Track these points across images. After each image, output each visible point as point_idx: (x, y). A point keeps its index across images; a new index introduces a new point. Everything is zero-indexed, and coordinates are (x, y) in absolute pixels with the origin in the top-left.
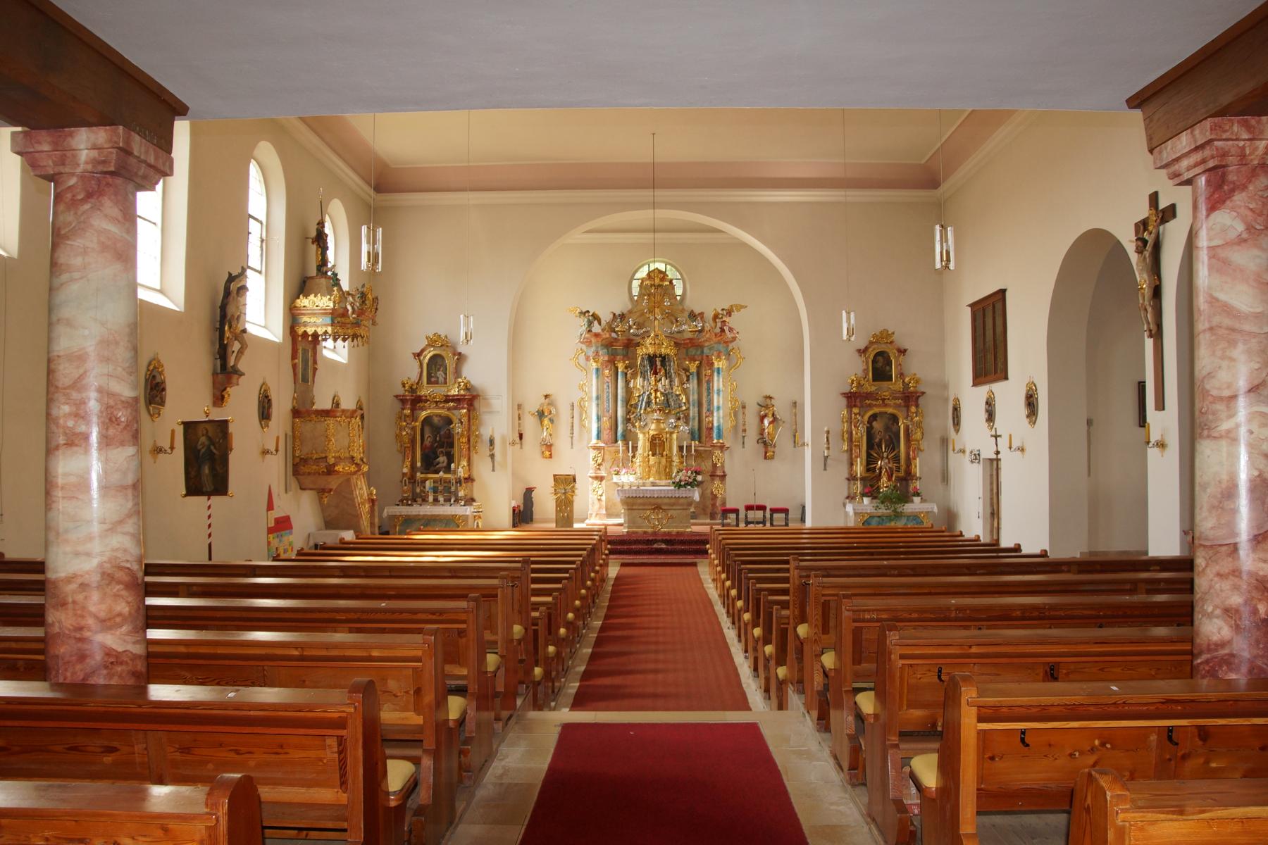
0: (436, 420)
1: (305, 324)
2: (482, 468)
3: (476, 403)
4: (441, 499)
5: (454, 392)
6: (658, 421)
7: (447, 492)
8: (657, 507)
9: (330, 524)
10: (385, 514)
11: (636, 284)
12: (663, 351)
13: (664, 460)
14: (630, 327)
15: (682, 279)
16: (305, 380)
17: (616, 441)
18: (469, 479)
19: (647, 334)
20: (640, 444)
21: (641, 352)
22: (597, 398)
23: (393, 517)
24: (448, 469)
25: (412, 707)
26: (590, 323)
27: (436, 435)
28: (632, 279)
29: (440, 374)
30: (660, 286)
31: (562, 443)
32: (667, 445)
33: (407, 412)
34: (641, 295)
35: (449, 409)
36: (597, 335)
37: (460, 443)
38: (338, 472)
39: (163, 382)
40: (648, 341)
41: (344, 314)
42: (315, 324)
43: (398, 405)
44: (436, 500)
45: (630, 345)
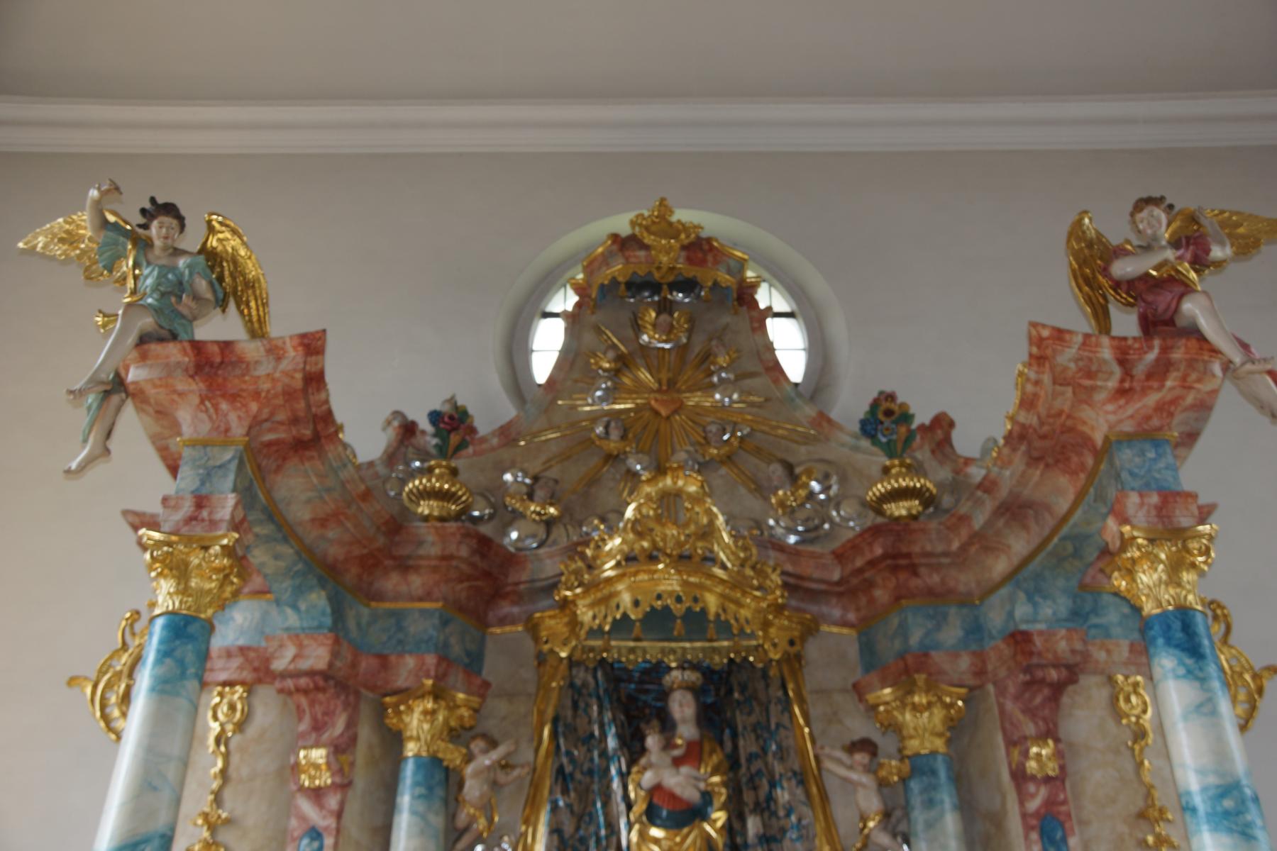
15: (806, 311)
34: (569, 359)
36: (212, 365)
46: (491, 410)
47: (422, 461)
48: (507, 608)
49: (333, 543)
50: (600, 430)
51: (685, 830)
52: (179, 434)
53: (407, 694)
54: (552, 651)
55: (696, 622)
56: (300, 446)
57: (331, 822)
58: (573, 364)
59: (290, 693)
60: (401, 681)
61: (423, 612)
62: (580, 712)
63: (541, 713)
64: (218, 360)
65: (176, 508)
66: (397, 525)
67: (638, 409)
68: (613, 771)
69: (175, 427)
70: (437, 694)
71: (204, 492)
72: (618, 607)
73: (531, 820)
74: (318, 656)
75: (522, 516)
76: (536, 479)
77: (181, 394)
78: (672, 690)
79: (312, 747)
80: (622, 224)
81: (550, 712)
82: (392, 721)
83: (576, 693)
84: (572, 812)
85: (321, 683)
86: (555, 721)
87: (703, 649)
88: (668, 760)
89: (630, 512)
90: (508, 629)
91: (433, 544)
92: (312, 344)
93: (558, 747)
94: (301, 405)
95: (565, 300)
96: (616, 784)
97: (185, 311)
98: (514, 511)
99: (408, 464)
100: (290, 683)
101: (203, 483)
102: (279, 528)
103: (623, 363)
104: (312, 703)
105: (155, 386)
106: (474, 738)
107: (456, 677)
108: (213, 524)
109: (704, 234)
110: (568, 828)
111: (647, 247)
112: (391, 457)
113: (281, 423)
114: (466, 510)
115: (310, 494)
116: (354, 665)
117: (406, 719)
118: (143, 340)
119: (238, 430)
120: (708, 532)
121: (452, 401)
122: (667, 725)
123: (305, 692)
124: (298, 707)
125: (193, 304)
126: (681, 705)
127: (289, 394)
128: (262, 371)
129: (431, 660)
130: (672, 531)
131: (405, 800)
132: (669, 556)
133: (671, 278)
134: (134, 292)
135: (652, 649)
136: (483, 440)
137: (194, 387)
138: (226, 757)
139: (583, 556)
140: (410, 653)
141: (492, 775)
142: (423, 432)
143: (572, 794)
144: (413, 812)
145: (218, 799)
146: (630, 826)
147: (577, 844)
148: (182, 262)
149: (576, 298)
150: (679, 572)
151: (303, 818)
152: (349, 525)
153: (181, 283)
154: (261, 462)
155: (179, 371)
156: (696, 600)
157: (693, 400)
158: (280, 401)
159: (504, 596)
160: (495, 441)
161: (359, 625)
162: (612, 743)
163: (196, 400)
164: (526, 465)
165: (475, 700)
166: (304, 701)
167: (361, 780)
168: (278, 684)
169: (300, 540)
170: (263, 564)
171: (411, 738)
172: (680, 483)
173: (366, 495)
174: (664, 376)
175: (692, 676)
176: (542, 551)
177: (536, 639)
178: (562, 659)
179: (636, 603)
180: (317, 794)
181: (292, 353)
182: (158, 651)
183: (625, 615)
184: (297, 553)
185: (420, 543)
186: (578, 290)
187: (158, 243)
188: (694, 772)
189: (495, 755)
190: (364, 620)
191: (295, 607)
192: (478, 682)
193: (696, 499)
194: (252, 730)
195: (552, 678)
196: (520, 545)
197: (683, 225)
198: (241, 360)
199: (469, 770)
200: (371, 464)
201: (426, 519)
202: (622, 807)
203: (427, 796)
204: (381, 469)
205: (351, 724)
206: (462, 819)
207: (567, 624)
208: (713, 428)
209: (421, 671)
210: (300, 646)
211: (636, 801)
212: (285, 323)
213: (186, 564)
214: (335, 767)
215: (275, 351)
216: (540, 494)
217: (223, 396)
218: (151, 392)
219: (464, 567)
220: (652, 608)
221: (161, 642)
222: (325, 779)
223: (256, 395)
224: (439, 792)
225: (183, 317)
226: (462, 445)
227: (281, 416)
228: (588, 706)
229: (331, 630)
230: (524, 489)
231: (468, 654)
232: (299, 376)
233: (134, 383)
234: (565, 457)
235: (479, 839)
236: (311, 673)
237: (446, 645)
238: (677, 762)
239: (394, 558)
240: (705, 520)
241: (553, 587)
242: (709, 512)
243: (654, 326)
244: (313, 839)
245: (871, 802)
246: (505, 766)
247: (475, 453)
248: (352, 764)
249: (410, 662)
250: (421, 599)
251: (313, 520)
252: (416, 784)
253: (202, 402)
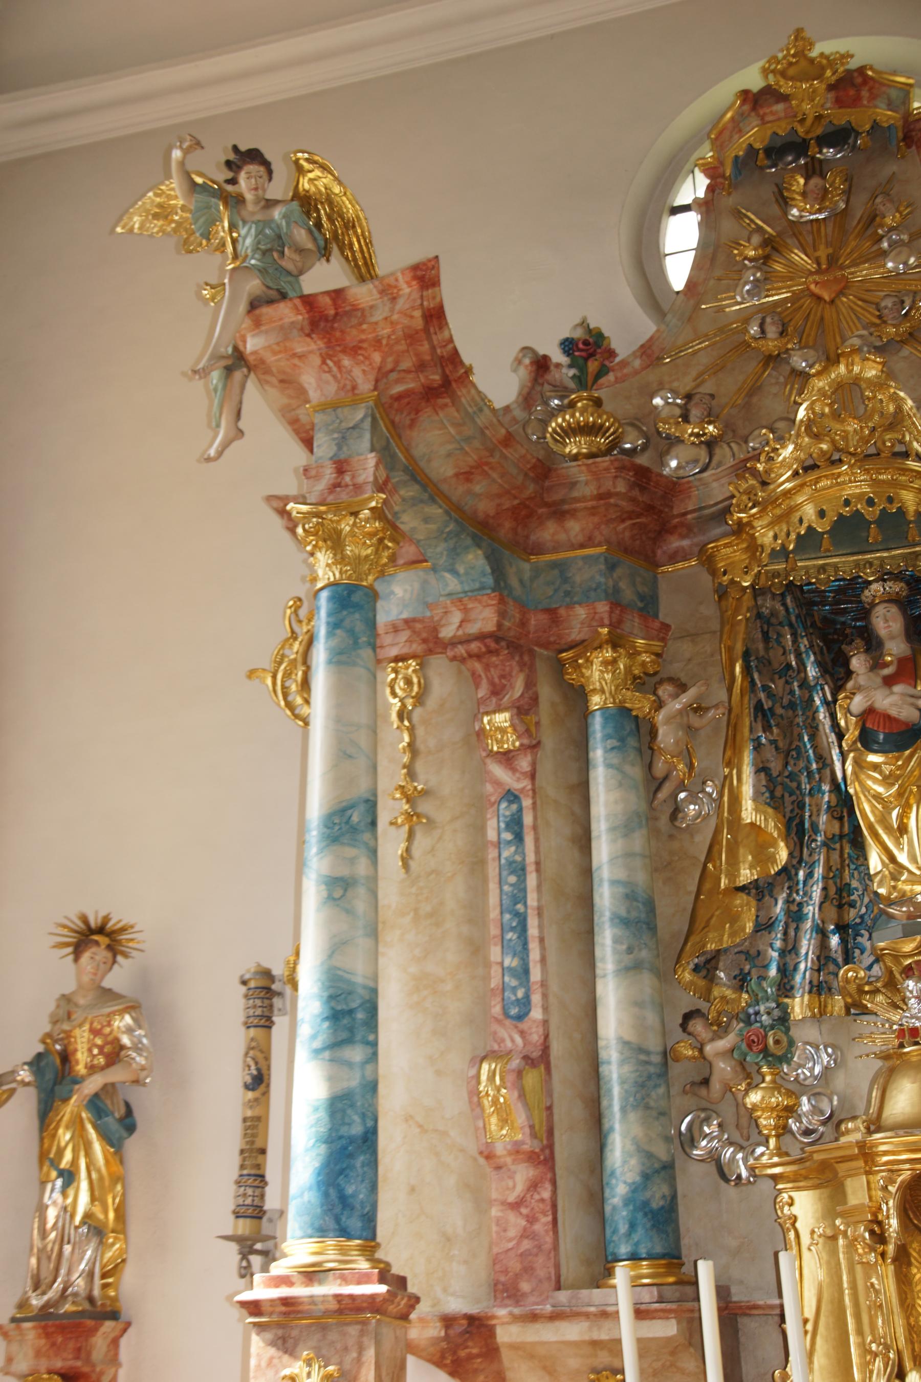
20: (804, 1281)
28: (658, 206)
34: (709, 255)
36: (327, 319)
46: (628, 328)
47: (561, 398)
48: (676, 543)
49: (481, 497)
50: (754, 330)
51: (907, 752)
52: (308, 401)
53: (582, 646)
54: (732, 582)
55: (894, 524)
56: (431, 394)
57: (526, 783)
58: (713, 259)
59: (463, 660)
60: (576, 633)
61: (585, 558)
62: (773, 644)
63: (730, 650)
64: (332, 312)
65: (318, 477)
66: (544, 469)
67: (796, 298)
68: (818, 702)
69: (301, 393)
70: (615, 643)
71: (342, 457)
72: (801, 521)
73: (733, 762)
74: (485, 618)
75: (680, 441)
76: (688, 397)
77: (301, 357)
78: (873, 605)
79: (494, 712)
80: (752, 78)
81: (739, 648)
82: (572, 676)
83: (765, 624)
84: (777, 748)
85: (493, 645)
86: (746, 655)
87: (904, 557)
88: (879, 680)
89: (801, 413)
90: (680, 565)
91: (587, 483)
92: (426, 275)
93: (753, 682)
94: (426, 347)
95: (694, 187)
96: (822, 715)
97: (290, 266)
98: (668, 437)
99: (546, 403)
100: (461, 650)
101: (340, 447)
102: (424, 487)
103: (771, 247)
104: (487, 667)
105: (275, 353)
106: (661, 682)
107: (633, 623)
108: (358, 488)
109: (853, 64)
110: (775, 766)
111: (785, 98)
112: (527, 399)
113: (408, 371)
114: (615, 444)
115: (450, 447)
116: (523, 623)
117: (587, 673)
118: (254, 305)
119: (365, 385)
120: (897, 421)
121: (583, 324)
122: (872, 644)
123: (478, 657)
124: (473, 674)
125: (296, 257)
126: (886, 621)
127: (411, 337)
128: (378, 316)
129: (603, 608)
130: (852, 426)
131: (598, 754)
132: (853, 455)
133: (819, 131)
134: (236, 256)
135: (843, 563)
136: (624, 364)
137: (313, 347)
138: (411, 730)
139: (754, 473)
140: (580, 604)
141: (685, 719)
142: (558, 365)
143: (775, 730)
144: (609, 766)
145: (411, 774)
146: (843, 756)
147: (787, 780)
148: (277, 213)
149: (707, 181)
150: (867, 471)
151: (497, 783)
152: (495, 475)
153: (279, 237)
154: (395, 416)
155: (295, 332)
156: (890, 500)
157: (863, 273)
158: (402, 347)
159: (671, 531)
160: (637, 363)
161: (521, 581)
162: (812, 672)
163: (317, 361)
164: (676, 384)
165: (657, 645)
166: (478, 666)
167: (549, 740)
168: (450, 653)
169: (447, 498)
170: (413, 529)
171: (594, 690)
172: (856, 369)
173: (508, 440)
174: (823, 253)
175: (894, 587)
176: (705, 475)
177: (713, 572)
178: (747, 587)
179: (822, 514)
180: (507, 758)
181: (406, 290)
182: (328, 623)
183: (810, 529)
184: (447, 513)
185: (573, 485)
186: (711, 171)
187: (249, 196)
188: (910, 690)
189: (685, 698)
190: (527, 576)
191: (454, 571)
192: (657, 625)
193: (878, 385)
194: (432, 702)
195: (737, 611)
196: (681, 473)
197: (827, 58)
198: (355, 308)
199: (660, 717)
200: (507, 409)
201: (575, 458)
202: (833, 738)
203: (621, 746)
204: (518, 413)
205: (530, 684)
206: (660, 768)
207: (747, 549)
208: (888, 303)
209: (594, 621)
210: (465, 610)
211: (848, 730)
212: (393, 257)
213: (339, 533)
214: (521, 729)
215: (389, 292)
216: (695, 413)
217: (344, 351)
218: (270, 359)
219: (623, 503)
220: (841, 516)
221: (329, 615)
222: (511, 741)
223: (377, 343)
224: (632, 742)
225: (289, 273)
226: (602, 372)
227: (406, 364)
228: (779, 635)
229: (494, 590)
230: (678, 411)
231: (642, 598)
232: (418, 314)
233: (255, 353)
234: (718, 368)
235: (682, 787)
236: (481, 637)
237: (617, 590)
238: (889, 682)
239: (547, 505)
240: (892, 408)
241: (727, 511)
242: (895, 398)
243: (804, 194)
244: (510, 802)
246: (698, 709)
247: (617, 380)
248: (537, 724)
249: (581, 612)
250: (582, 546)
251: (457, 475)
252: (607, 737)
253: (324, 362)
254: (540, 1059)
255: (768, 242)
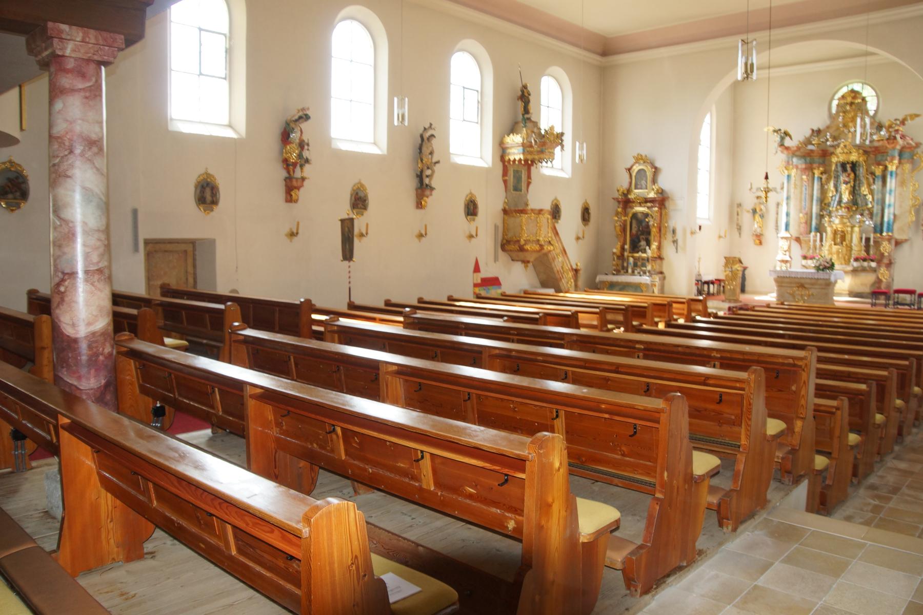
0: (640, 216)
1: (509, 154)
2: (669, 250)
3: (667, 204)
4: (636, 272)
5: (652, 195)
6: (842, 217)
7: (639, 265)
8: (802, 286)
9: (544, 285)
10: (598, 279)
11: (835, 103)
12: (854, 157)
13: (844, 249)
14: (827, 140)
16: (517, 188)
17: (811, 232)
18: (660, 258)
19: (838, 145)
21: (834, 160)
22: (788, 198)
23: (603, 282)
24: (644, 251)
25: (736, 429)
26: (782, 139)
27: (636, 225)
28: (832, 99)
29: (643, 182)
30: (851, 104)
31: (769, 234)
32: (848, 237)
33: (620, 210)
34: (838, 112)
35: (648, 208)
36: (787, 148)
37: (654, 231)
38: (527, 250)
39: (366, 196)
40: (839, 150)
41: (531, 146)
42: (514, 154)
43: (616, 204)
44: (633, 272)
45: (825, 154)
74: (804, 166)
245: (871, 181)
254: (807, 214)
255: (844, 112)
